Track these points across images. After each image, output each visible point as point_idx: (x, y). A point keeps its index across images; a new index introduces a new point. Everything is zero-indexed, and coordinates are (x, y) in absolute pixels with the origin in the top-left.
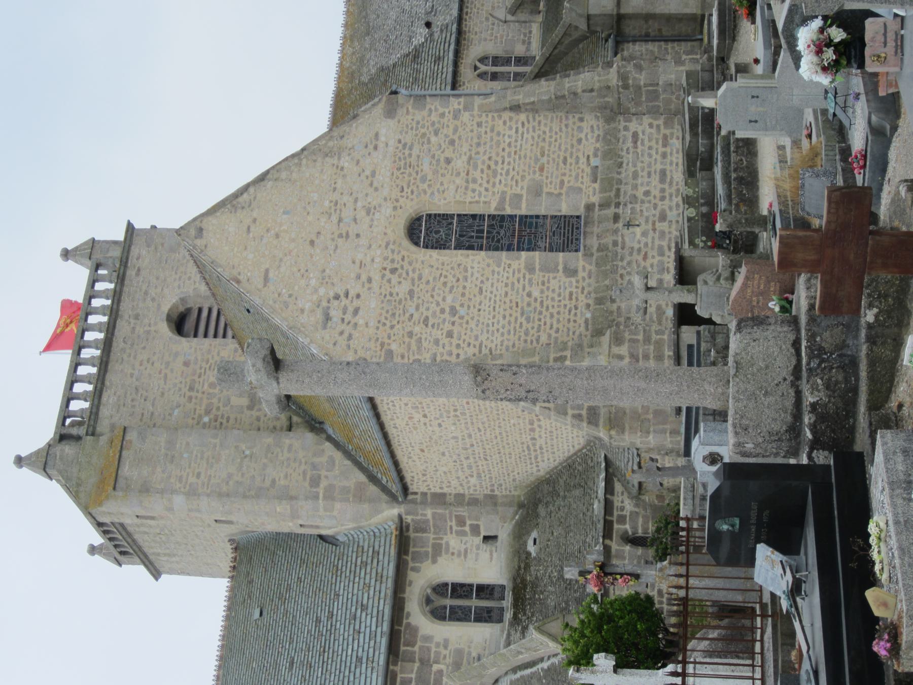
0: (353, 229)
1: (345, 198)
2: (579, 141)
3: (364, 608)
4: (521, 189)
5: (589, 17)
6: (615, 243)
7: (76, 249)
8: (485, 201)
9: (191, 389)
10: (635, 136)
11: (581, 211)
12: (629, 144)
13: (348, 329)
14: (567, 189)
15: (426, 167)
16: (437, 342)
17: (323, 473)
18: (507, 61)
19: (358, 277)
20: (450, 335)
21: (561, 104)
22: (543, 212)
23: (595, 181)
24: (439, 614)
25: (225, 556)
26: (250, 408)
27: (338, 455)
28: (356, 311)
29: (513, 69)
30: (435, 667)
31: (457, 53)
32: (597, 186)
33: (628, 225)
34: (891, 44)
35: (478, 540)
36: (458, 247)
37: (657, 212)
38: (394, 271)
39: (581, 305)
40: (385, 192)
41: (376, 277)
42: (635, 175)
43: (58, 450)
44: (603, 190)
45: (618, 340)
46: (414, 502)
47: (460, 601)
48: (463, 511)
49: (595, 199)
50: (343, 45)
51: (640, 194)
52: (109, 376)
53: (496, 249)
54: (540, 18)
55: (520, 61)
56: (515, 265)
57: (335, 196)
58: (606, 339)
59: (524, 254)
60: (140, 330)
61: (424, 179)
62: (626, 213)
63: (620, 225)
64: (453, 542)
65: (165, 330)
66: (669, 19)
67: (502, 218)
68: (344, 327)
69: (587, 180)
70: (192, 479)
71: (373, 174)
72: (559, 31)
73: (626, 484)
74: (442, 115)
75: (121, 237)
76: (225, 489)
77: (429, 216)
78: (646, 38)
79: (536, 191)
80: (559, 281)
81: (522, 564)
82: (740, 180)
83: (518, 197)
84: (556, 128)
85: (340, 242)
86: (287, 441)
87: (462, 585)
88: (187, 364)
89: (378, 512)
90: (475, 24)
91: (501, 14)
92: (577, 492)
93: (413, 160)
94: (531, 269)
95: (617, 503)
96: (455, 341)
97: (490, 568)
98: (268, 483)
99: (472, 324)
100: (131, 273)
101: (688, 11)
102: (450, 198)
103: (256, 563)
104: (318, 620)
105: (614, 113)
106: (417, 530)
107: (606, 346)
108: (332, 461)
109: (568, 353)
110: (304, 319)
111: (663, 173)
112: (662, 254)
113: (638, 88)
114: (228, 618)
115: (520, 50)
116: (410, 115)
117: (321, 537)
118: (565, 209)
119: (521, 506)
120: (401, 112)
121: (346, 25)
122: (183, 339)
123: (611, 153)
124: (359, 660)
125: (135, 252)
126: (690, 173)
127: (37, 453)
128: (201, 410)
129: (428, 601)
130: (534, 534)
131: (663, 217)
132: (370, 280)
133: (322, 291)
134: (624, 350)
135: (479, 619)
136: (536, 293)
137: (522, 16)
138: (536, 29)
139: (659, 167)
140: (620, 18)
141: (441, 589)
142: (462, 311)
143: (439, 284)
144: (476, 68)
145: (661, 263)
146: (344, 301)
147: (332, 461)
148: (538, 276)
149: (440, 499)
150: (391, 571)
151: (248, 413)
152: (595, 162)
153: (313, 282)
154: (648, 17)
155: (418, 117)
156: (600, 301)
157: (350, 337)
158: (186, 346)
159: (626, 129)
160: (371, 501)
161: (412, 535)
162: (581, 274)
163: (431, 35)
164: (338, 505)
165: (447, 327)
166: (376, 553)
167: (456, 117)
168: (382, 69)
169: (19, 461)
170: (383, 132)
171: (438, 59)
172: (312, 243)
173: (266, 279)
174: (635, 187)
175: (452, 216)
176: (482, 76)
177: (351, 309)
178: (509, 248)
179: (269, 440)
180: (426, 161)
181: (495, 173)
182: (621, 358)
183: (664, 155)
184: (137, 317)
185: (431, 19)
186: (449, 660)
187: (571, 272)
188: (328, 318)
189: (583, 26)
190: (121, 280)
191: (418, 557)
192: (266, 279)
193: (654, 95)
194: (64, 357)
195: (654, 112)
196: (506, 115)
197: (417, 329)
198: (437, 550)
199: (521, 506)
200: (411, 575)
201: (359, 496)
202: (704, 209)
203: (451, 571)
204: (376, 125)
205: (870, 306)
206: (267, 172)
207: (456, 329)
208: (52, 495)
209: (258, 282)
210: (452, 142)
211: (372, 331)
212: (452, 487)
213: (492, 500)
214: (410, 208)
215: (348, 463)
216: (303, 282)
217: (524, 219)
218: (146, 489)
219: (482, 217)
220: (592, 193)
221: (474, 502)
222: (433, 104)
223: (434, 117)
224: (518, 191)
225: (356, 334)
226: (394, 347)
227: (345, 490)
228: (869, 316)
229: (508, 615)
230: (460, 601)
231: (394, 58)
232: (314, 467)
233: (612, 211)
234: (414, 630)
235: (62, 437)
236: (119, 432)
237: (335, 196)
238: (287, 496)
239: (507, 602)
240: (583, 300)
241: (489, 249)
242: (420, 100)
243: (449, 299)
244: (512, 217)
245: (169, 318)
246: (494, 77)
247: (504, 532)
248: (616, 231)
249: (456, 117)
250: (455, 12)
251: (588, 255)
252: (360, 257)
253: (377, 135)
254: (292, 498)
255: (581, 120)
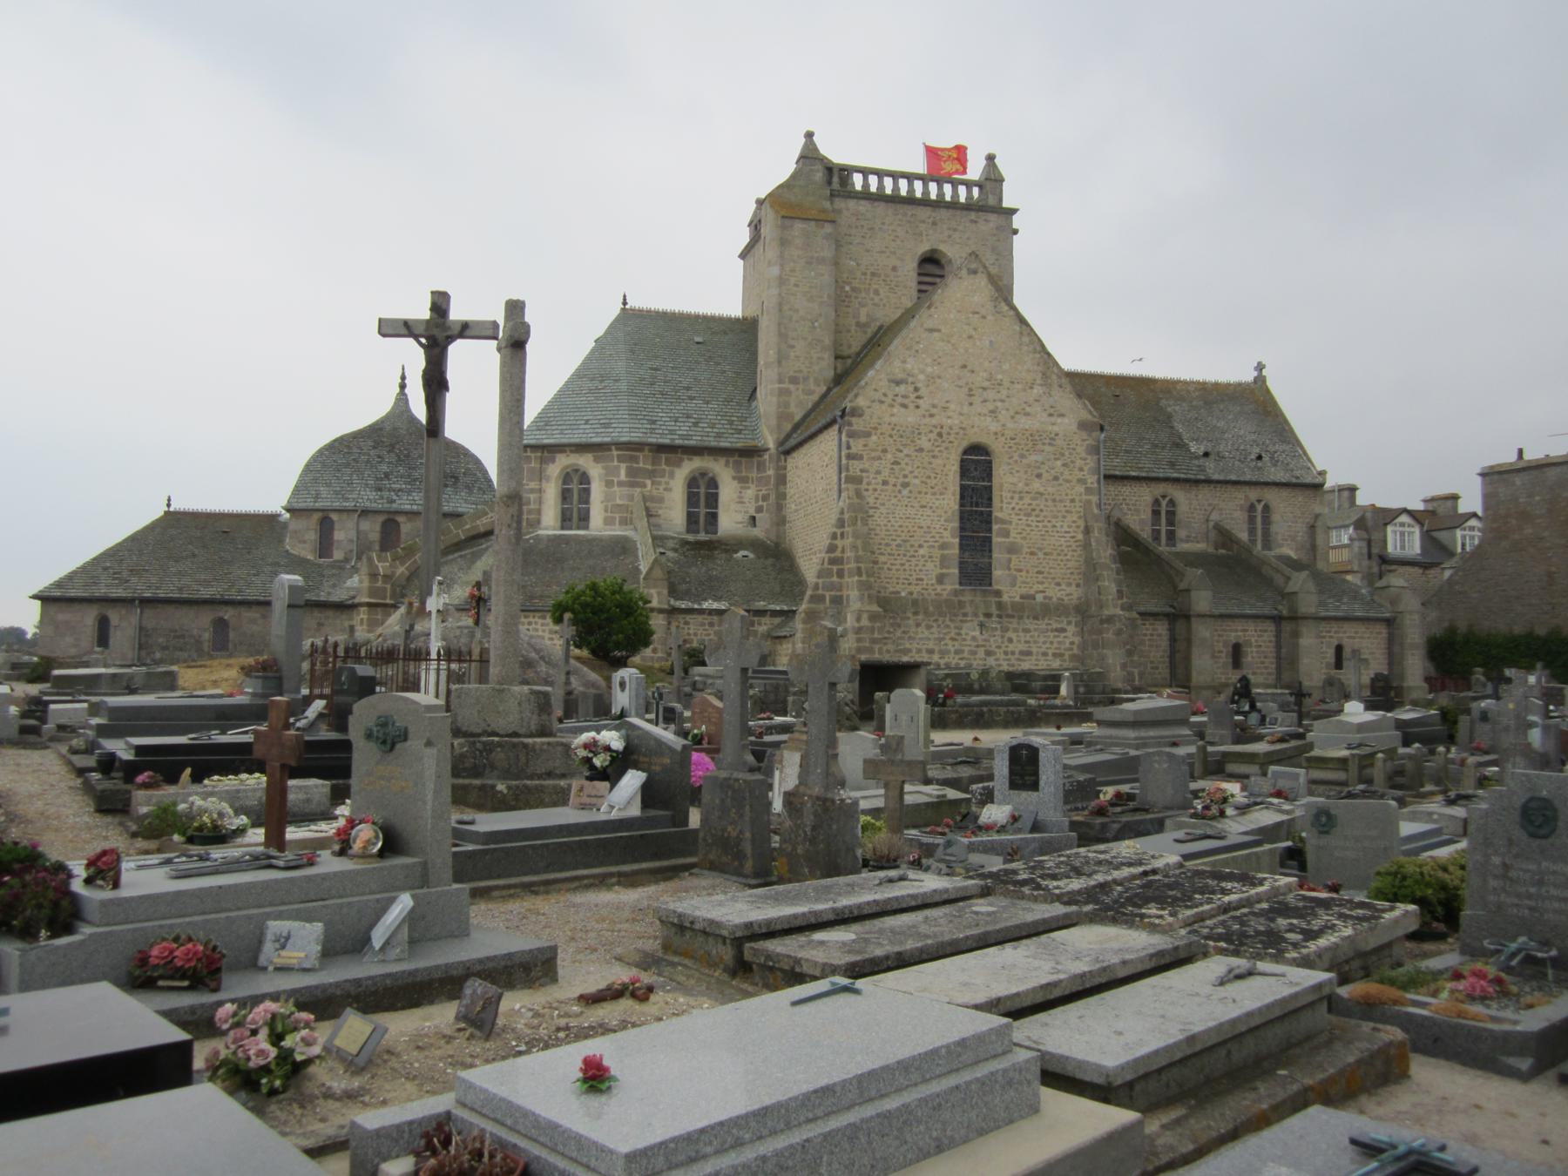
0: (977, 400)
1: (1004, 392)
2: (1058, 584)
3: (695, 424)
4: (1014, 537)
5: (1188, 591)
6: (965, 615)
7: (995, 166)
8: (1004, 507)
9: (873, 274)
10: (1063, 630)
11: (995, 587)
12: (1055, 626)
13: (888, 400)
14: (1013, 577)
15: (1033, 458)
16: (878, 472)
17: (801, 387)
18: (1171, 522)
19: (934, 406)
20: (885, 483)
21: (1090, 571)
22: (995, 555)
23: (1022, 597)
24: (692, 483)
25: (750, 313)
26: (858, 324)
27: (815, 397)
28: (904, 406)
29: (1164, 528)
30: (648, 482)
31: (1176, 480)
32: (1017, 599)
33: (982, 625)
34: (588, 800)
35: (752, 512)
36: (963, 488)
37: (993, 648)
38: (940, 435)
39: (912, 588)
40: (1010, 425)
41: (934, 421)
42: (1027, 631)
43: (819, 167)
44: (1014, 605)
45: (873, 617)
46: (779, 460)
47: (702, 496)
48: (772, 498)
49: (1005, 598)
50: (1198, 383)
51: (1010, 634)
52: (883, 205)
53: (961, 518)
54: (1211, 550)
55: (1171, 536)
56: (947, 534)
57: (1006, 384)
58: (875, 608)
59: (957, 540)
60: (922, 227)
61: (1022, 456)
62: (993, 623)
63: (982, 618)
64: (750, 493)
65: (924, 248)
66: (1187, 659)
67: (990, 522)
68: (890, 396)
69: (1024, 591)
70: (793, 280)
71: (1027, 414)
72: (1179, 565)
73: (780, 626)
74: (1081, 469)
75: (1005, 205)
76: (785, 308)
77: (990, 462)
78: (1173, 640)
79: (1013, 549)
80: (933, 569)
81: (729, 546)
82: (981, 714)
83: (1007, 534)
84: (1070, 564)
85: (965, 390)
86: (826, 356)
87: (716, 501)
88: (894, 269)
89: (771, 433)
90: (1204, 495)
91: (1215, 517)
92: (778, 589)
93: (1040, 446)
94: (943, 546)
95: (763, 620)
96: (879, 487)
97: (730, 521)
98: (792, 342)
99: (894, 501)
100: (973, 215)
101: (1194, 674)
102: (1005, 478)
103: (738, 336)
104: (688, 389)
105: (1082, 611)
106: (759, 464)
107: (868, 608)
108: (811, 393)
109: (864, 578)
110: (897, 363)
111: (1029, 653)
112: (957, 652)
113: (1100, 632)
114: (697, 317)
115: (1181, 533)
116: (1081, 443)
117: (755, 390)
118: (997, 573)
119: (777, 545)
120: (1084, 435)
121: (1216, 385)
122: (915, 264)
123: (1047, 610)
124: (654, 422)
125: (993, 217)
126: (1010, 676)
127: (816, 150)
128: (856, 284)
129: (703, 474)
130: (751, 556)
131: (989, 653)
132: (932, 416)
133: (921, 377)
134: (865, 622)
135: (563, 512)
136: (921, 552)
137: (1213, 534)
138: (1200, 546)
139: (1034, 650)
140: (1187, 617)
141: (713, 483)
142: (905, 492)
143: (928, 473)
144: (1164, 497)
145: (948, 652)
146: (913, 396)
147: (811, 393)
148: (937, 553)
149: (782, 480)
150: (724, 444)
151: (854, 322)
152: (1039, 598)
153: (929, 369)
154: (1189, 641)
155: (1079, 449)
156: (915, 603)
157: (882, 402)
158: (909, 269)
159: (1069, 623)
160: (779, 426)
161: (755, 460)
162: (939, 588)
163: (1197, 458)
164: (775, 399)
165: (892, 480)
166: (740, 432)
167: (1079, 481)
168: (1170, 417)
169: (809, 135)
170: (1066, 420)
171: (1172, 464)
172: (964, 366)
173: (931, 330)
174: (1016, 630)
175: (990, 480)
176: (1157, 502)
177: (906, 401)
178: (962, 529)
179: (827, 341)
180: (1039, 458)
181: (1029, 515)
182: (858, 620)
183: (1045, 654)
184: (934, 224)
185: (1212, 457)
186: (655, 492)
187: (941, 579)
188: (898, 383)
189: (1182, 586)
190: (969, 207)
191: (737, 465)
192: (931, 330)
193: (1096, 645)
194: (920, 167)
195: (1083, 646)
196: (1081, 523)
197: (889, 456)
198: (742, 480)
199: (777, 545)
200: (722, 461)
201: (783, 416)
202: (976, 686)
203: (728, 490)
204: (1070, 415)
205: (509, 788)
206: (1027, 325)
207: (890, 487)
208: (783, 168)
209: (929, 324)
210: (1056, 478)
211: (887, 419)
212: (790, 490)
213: (781, 521)
214: (997, 446)
215: (810, 405)
216: (929, 361)
217: (989, 540)
218: (783, 243)
219: (990, 505)
220: (1010, 595)
221: (780, 507)
222: (1091, 462)
223: (1079, 463)
224: (1013, 534)
225: (884, 407)
226: (874, 438)
227: (787, 405)
228: (501, 787)
229: (690, 538)
230: (702, 496)
231: (1180, 428)
232: (806, 379)
233: (994, 610)
234: (678, 464)
235: (830, 169)
236: (831, 216)
237: (1006, 384)
238: (781, 359)
239: (702, 537)
240: (916, 589)
241: (962, 513)
242: (1095, 450)
243: (917, 481)
244: (990, 530)
245: (934, 251)
246: (1156, 513)
247: (757, 532)
248: (976, 615)
249: (1079, 481)
250: (1216, 477)
251: (955, 593)
252: (952, 406)
253: (1062, 415)
254: (779, 362)
255: (1078, 585)
